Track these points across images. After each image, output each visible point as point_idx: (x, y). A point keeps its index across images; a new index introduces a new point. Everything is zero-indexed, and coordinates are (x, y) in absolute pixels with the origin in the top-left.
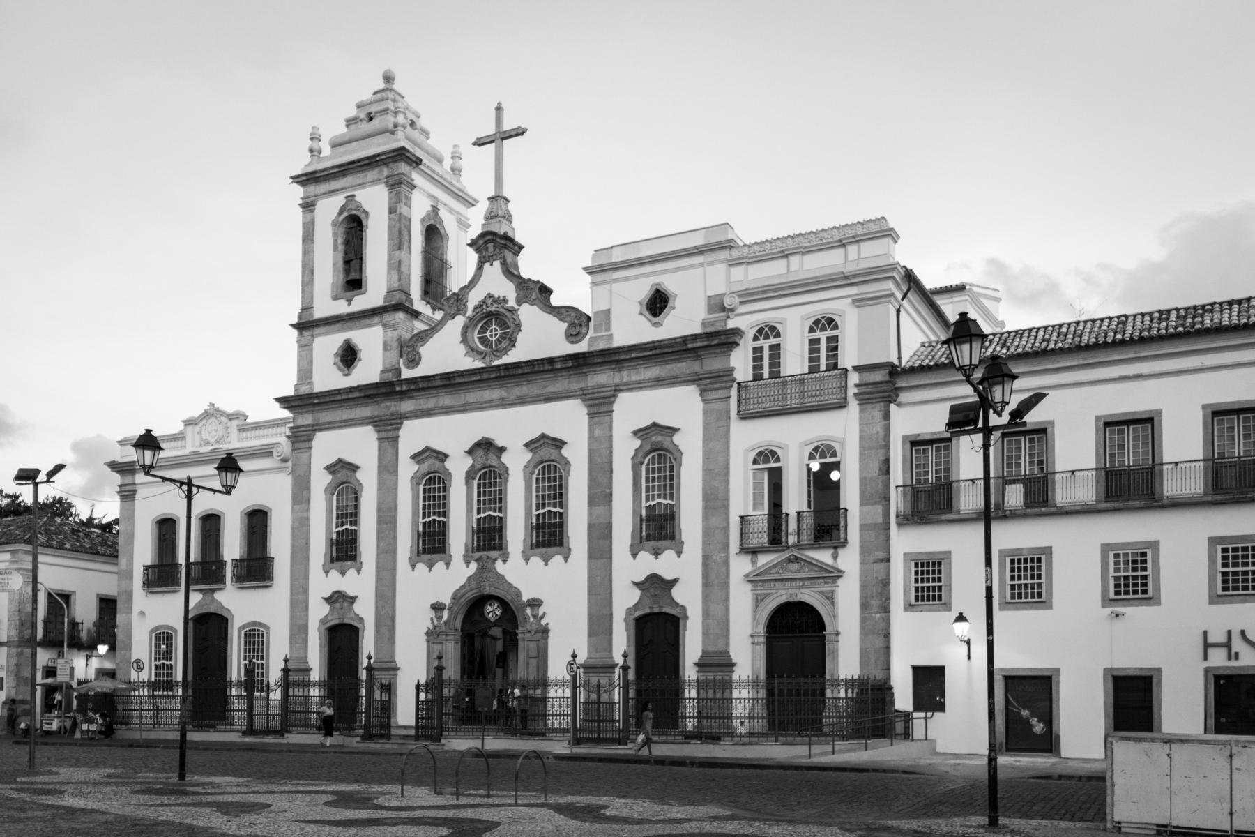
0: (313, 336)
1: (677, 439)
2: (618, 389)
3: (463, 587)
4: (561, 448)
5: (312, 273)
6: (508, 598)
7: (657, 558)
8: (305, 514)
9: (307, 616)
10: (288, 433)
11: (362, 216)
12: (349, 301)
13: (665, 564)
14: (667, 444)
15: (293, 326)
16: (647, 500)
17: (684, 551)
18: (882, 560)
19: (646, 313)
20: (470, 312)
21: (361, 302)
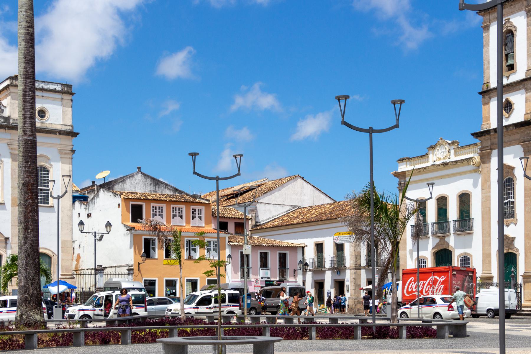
0: (490, 98)
5: (489, 63)
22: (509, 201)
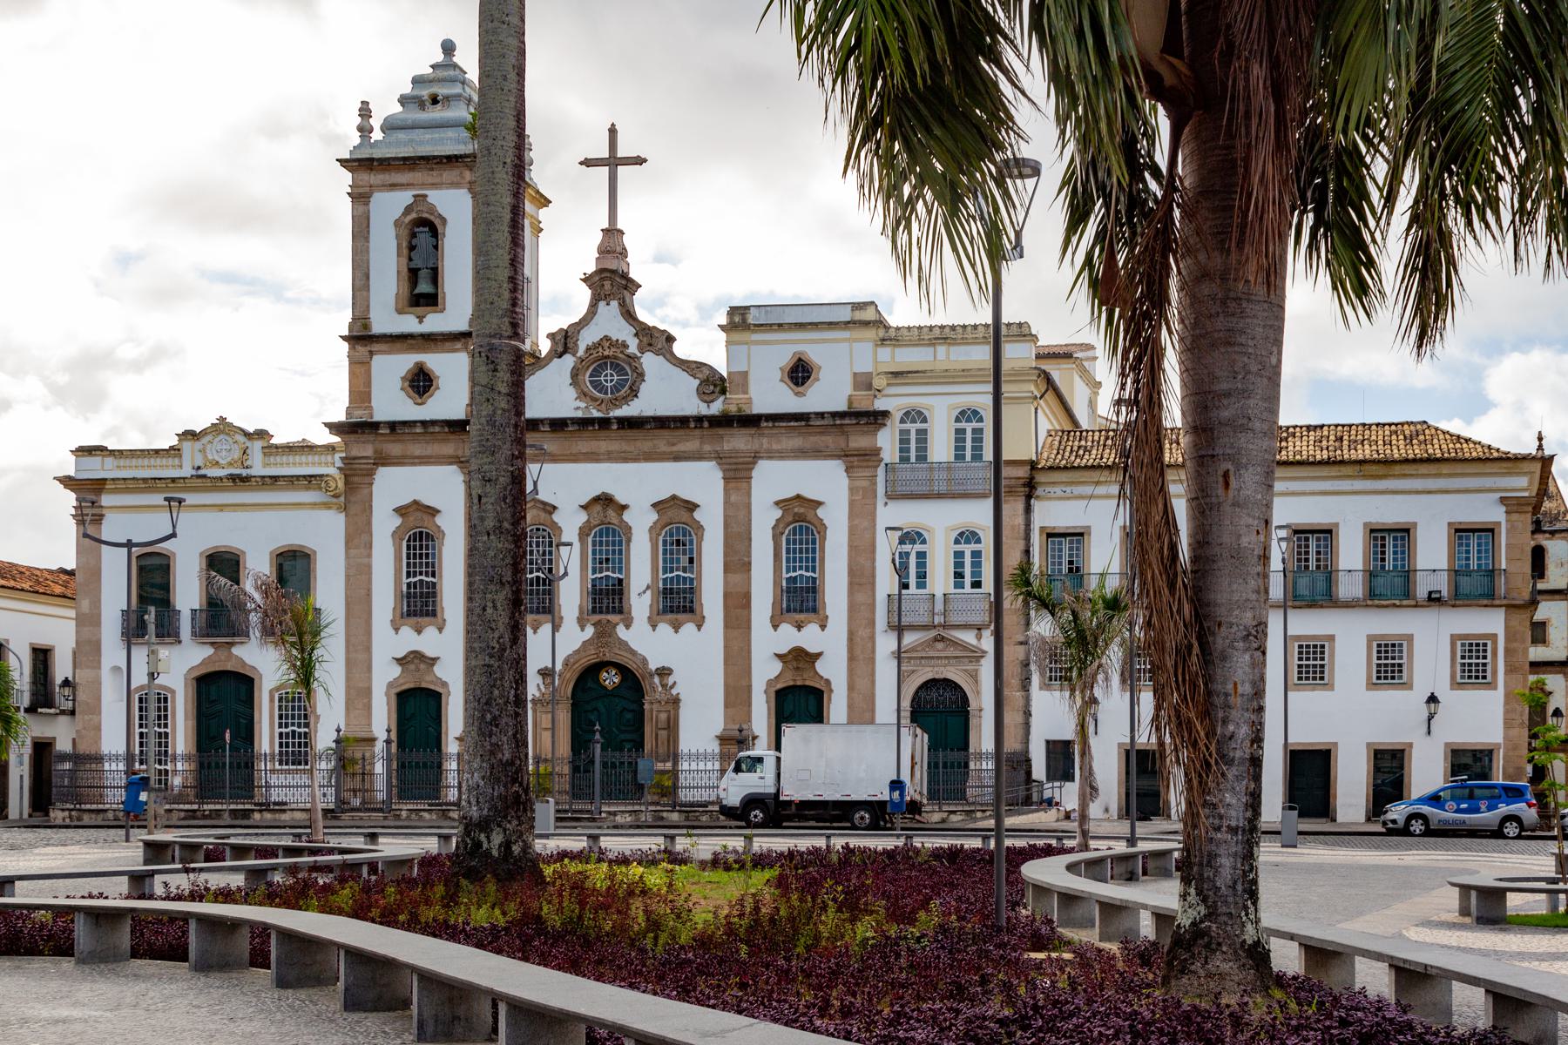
0: (371, 353)
1: (820, 512)
2: (756, 457)
3: (577, 652)
4: (693, 510)
5: (368, 278)
6: (632, 666)
8: (365, 561)
9: (370, 679)
10: (339, 464)
11: (437, 222)
12: (421, 319)
13: (809, 638)
14: (810, 517)
15: (344, 338)
16: (788, 572)
19: (787, 379)
20: (581, 353)
21: (434, 323)
22: (421, 581)
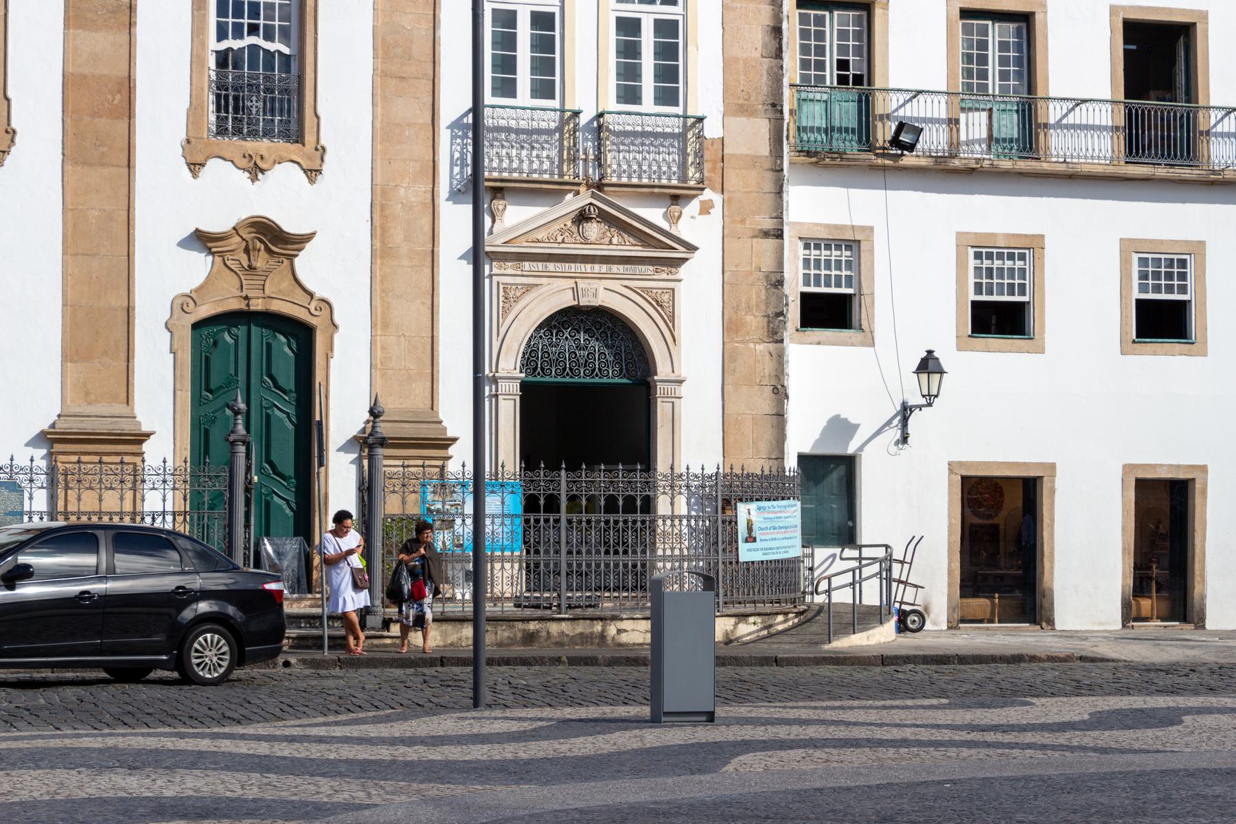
7: (254, 179)
17: (326, 168)
18: (766, 234)
